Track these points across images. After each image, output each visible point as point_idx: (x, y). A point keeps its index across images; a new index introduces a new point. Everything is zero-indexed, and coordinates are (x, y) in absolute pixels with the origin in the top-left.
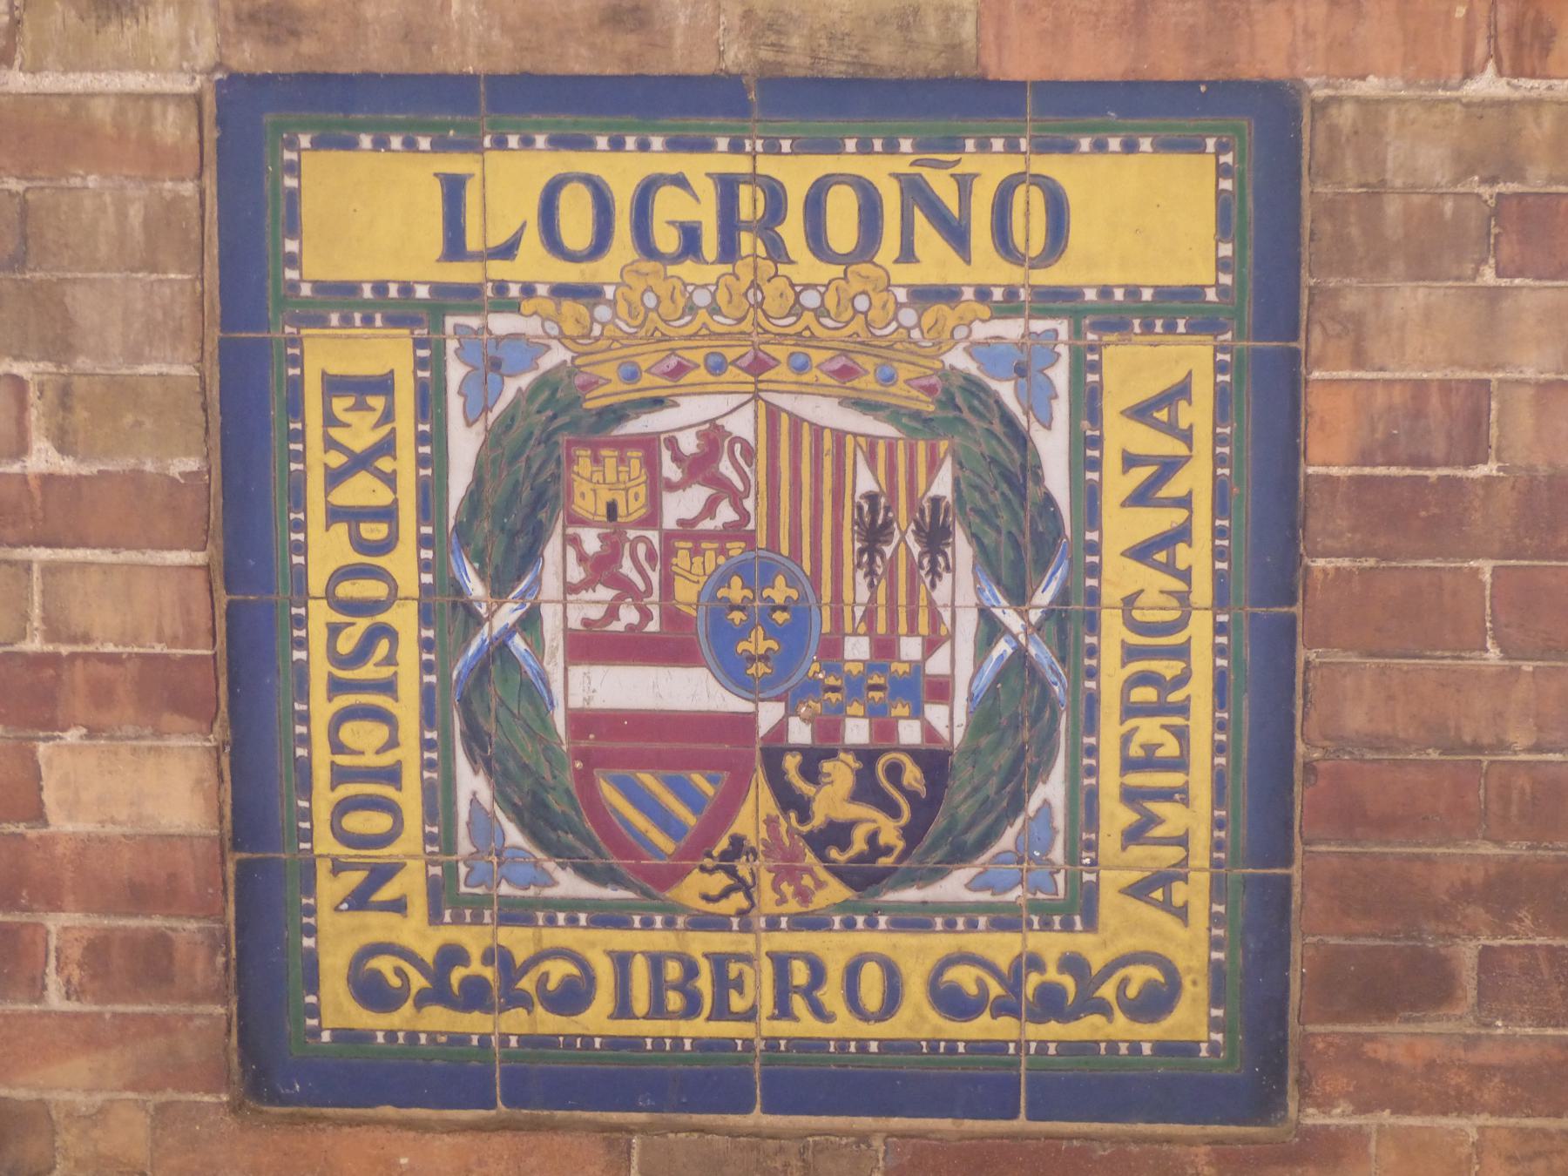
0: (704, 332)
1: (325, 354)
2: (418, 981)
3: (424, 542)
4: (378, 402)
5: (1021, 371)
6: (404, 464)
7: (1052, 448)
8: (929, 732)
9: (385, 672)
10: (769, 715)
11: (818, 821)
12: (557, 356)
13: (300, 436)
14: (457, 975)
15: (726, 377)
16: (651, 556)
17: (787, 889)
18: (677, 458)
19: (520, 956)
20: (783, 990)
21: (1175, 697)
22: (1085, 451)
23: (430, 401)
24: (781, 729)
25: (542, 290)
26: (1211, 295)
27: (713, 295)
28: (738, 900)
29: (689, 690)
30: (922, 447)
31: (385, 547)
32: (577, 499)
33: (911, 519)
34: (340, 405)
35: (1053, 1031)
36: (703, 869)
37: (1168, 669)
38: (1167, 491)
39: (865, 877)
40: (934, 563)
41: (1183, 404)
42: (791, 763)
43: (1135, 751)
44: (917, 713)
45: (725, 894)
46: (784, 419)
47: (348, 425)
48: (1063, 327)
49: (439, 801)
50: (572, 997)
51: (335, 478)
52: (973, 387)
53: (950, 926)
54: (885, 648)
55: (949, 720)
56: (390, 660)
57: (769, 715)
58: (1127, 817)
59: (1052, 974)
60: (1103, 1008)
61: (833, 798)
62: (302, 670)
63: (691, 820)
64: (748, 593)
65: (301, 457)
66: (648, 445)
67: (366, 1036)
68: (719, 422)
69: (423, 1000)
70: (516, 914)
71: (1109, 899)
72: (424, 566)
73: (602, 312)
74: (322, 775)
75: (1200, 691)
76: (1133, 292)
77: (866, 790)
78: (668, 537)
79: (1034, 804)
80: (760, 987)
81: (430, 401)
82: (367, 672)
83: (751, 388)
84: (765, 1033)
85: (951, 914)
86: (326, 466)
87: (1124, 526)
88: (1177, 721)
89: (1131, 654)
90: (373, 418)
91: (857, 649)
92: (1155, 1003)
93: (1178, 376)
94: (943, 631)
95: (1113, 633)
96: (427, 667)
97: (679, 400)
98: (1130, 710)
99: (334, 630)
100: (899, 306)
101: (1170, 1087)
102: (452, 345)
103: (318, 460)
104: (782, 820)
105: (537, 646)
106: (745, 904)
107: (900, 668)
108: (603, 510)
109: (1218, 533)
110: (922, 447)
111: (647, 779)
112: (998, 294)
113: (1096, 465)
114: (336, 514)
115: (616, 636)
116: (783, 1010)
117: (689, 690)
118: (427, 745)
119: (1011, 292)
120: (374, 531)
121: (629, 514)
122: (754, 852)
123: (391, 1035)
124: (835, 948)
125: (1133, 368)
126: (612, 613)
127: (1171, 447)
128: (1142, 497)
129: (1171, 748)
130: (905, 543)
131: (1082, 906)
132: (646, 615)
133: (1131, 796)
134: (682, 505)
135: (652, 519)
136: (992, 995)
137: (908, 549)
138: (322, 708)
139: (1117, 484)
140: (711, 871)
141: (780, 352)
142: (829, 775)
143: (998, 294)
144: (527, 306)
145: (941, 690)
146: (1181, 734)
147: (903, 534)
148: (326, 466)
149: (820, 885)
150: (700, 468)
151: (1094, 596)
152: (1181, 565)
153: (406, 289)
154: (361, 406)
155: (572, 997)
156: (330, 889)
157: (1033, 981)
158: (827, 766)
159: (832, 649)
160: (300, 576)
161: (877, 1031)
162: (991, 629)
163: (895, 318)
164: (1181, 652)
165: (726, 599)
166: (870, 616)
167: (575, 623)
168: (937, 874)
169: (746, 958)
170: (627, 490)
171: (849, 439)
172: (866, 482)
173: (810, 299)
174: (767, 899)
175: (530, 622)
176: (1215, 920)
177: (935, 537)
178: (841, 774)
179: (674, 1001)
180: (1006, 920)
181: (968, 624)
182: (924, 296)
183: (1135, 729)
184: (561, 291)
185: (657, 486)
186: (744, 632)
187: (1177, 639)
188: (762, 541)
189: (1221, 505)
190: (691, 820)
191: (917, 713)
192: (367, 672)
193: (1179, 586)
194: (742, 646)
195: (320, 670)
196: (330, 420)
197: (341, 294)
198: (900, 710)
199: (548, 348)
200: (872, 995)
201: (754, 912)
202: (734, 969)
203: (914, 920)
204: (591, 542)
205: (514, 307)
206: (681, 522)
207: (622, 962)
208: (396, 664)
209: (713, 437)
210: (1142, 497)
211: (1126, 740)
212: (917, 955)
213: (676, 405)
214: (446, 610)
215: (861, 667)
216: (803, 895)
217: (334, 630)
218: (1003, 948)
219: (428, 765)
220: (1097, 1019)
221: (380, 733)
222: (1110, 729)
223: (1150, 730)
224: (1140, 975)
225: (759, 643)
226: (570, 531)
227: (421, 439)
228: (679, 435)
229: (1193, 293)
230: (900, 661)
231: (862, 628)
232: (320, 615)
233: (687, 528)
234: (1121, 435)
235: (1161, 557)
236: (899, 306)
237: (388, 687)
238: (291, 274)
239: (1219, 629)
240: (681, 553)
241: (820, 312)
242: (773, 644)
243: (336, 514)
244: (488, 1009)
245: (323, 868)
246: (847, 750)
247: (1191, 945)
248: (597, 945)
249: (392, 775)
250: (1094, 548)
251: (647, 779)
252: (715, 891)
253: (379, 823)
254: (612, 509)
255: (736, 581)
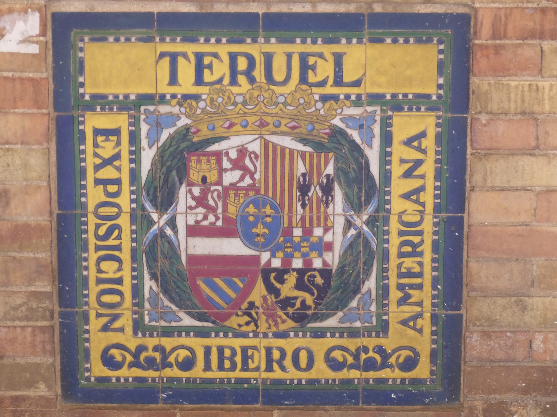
0: (241, 112)
1: (93, 121)
2: (129, 358)
3: (132, 192)
4: (114, 138)
5: (361, 127)
6: (125, 163)
7: (373, 155)
8: (325, 263)
9: (116, 242)
10: (265, 256)
11: (282, 296)
12: (184, 121)
13: (84, 152)
14: (143, 356)
15: (248, 128)
16: (218, 196)
17: (270, 321)
18: (229, 160)
19: (168, 349)
20: (269, 361)
21: (418, 250)
22: (385, 157)
23: (134, 138)
24: (269, 262)
25: (179, 96)
26: (434, 98)
27: (244, 97)
28: (252, 327)
29: (234, 247)
30: (323, 155)
31: (116, 194)
32: (191, 176)
33: (318, 183)
34: (100, 139)
35: (372, 375)
36: (237, 315)
37: (416, 239)
38: (416, 173)
39: (300, 318)
40: (327, 199)
41: (423, 139)
42: (273, 275)
43: (403, 270)
44: (320, 255)
45: (247, 324)
46: (271, 145)
47: (103, 147)
48: (378, 108)
49: (137, 291)
50: (187, 364)
51: (97, 168)
52: (342, 132)
53: (333, 336)
54: (307, 233)
55: (333, 259)
56: (119, 237)
57: (265, 256)
58: (400, 294)
59: (371, 354)
60: (391, 367)
61: (288, 289)
62: (86, 241)
63: (233, 295)
64: (256, 210)
65: (84, 160)
66: (218, 155)
67: (107, 379)
68: (245, 146)
69: (131, 365)
70: (167, 333)
71: (393, 326)
72: (132, 201)
73: (202, 104)
74: (92, 282)
75: (427, 248)
76: (405, 95)
77: (300, 286)
78: (226, 189)
79: (364, 289)
80: (259, 359)
81: (134, 138)
82: (111, 242)
83: (259, 132)
84: (262, 377)
85: (333, 332)
86: (94, 163)
87: (399, 186)
88: (419, 259)
89: (401, 233)
90: (113, 144)
91: (297, 232)
92: (410, 364)
93: (421, 129)
94: (329, 224)
95: (394, 226)
96: (133, 240)
97: (231, 137)
98: (401, 255)
99: (98, 226)
100: (316, 101)
101: (410, 396)
102: (143, 117)
103: (90, 162)
104: (268, 297)
105: (176, 232)
106: (255, 328)
107: (313, 239)
108: (200, 180)
109: (436, 188)
110: (323, 155)
111: (218, 281)
112: (353, 98)
113: (390, 163)
114: (98, 182)
115: (205, 227)
116: (269, 368)
117: (234, 247)
118: (133, 269)
119: (359, 97)
120: (112, 189)
121: (211, 182)
122: (258, 308)
123: (118, 379)
124: (290, 344)
125: (405, 125)
126: (205, 217)
127: (418, 156)
128: (408, 174)
129: (417, 269)
130: (315, 192)
131: (383, 328)
132: (217, 219)
133: (401, 287)
134: (230, 177)
135: (219, 183)
136: (349, 363)
137: (317, 193)
138: (93, 256)
139: (397, 170)
140: (242, 316)
141: (268, 119)
142: (287, 279)
143: (353, 98)
144: (174, 102)
145: (329, 247)
146: (421, 264)
147: (315, 188)
148: (94, 163)
149: (284, 322)
150: (237, 164)
151: (389, 211)
152: (421, 200)
153: (126, 97)
154: (107, 140)
155: (187, 364)
156: (95, 324)
157: (363, 356)
158: (286, 277)
159: (288, 232)
160: (84, 206)
161: (304, 376)
162: (349, 224)
163: (315, 105)
164: (421, 233)
165: (248, 212)
166: (303, 219)
167: (191, 222)
168: (326, 317)
169: (255, 348)
170: (210, 172)
171: (296, 152)
172: (301, 168)
173: (281, 99)
174: (263, 326)
175: (172, 223)
176: (433, 333)
177: (327, 190)
178: (291, 279)
179: (227, 364)
180: (353, 333)
181: (339, 223)
182: (325, 98)
183: (403, 262)
184: (186, 97)
185: (221, 171)
186: (255, 224)
187: (418, 229)
188: (263, 192)
189: (437, 177)
190: (233, 295)
191: (320, 255)
192: (111, 242)
193: (421, 208)
194: (254, 230)
195: (92, 242)
196: (96, 145)
197: (99, 98)
198: (314, 254)
199: (180, 118)
200: (303, 363)
201: (258, 330)
202: (250, 352)
203: (319, 334)
204: (196, 191)
205: (168, 103)
206: (231, 184)
207: (208, 351)
208: (121, 239)
209: (242, 151)
210: (408, 174)
211: (400, 266)
212: (320, 346)
213: (229, 139)
214: (140, 219)
215: (299, 239)
216: (276, 325)
217: (98, 226)
218: (352, 344)
219: (133, 278)
220: (388, 370)
221: (115, 265)
222: (394, 261)
223: (409, 263)
224: (405, 353)
225: (260, 229)
226: (188, 188)
227: (131, 153)
228: (230, 151)
229: (428, 96)
230: (313, 236)
231: (299, 224)
232: (92, 220)
233: (233, 186)
234: (399, 151)
235: (414, 197)
236: (316, 101)
237: (118, 248)
238: (81, 90)
239: (435, 224)
240: (231, 195)
241: (285, 104)
242: (266, 231)
243: (98, 182)
244: (157, 370)
245: (92, 315)
246: (294, 270)
247: (425, 344)
248: (197, 344)
249: (119, 281)
250: (389, 193)
251: (218, 281)
252: (242, 323)
253: (115, 299)
254: (204, 179)
255: (251, 206)
